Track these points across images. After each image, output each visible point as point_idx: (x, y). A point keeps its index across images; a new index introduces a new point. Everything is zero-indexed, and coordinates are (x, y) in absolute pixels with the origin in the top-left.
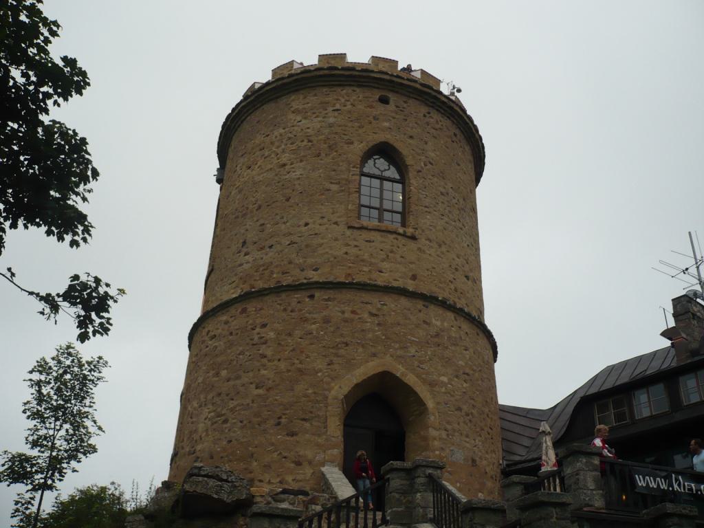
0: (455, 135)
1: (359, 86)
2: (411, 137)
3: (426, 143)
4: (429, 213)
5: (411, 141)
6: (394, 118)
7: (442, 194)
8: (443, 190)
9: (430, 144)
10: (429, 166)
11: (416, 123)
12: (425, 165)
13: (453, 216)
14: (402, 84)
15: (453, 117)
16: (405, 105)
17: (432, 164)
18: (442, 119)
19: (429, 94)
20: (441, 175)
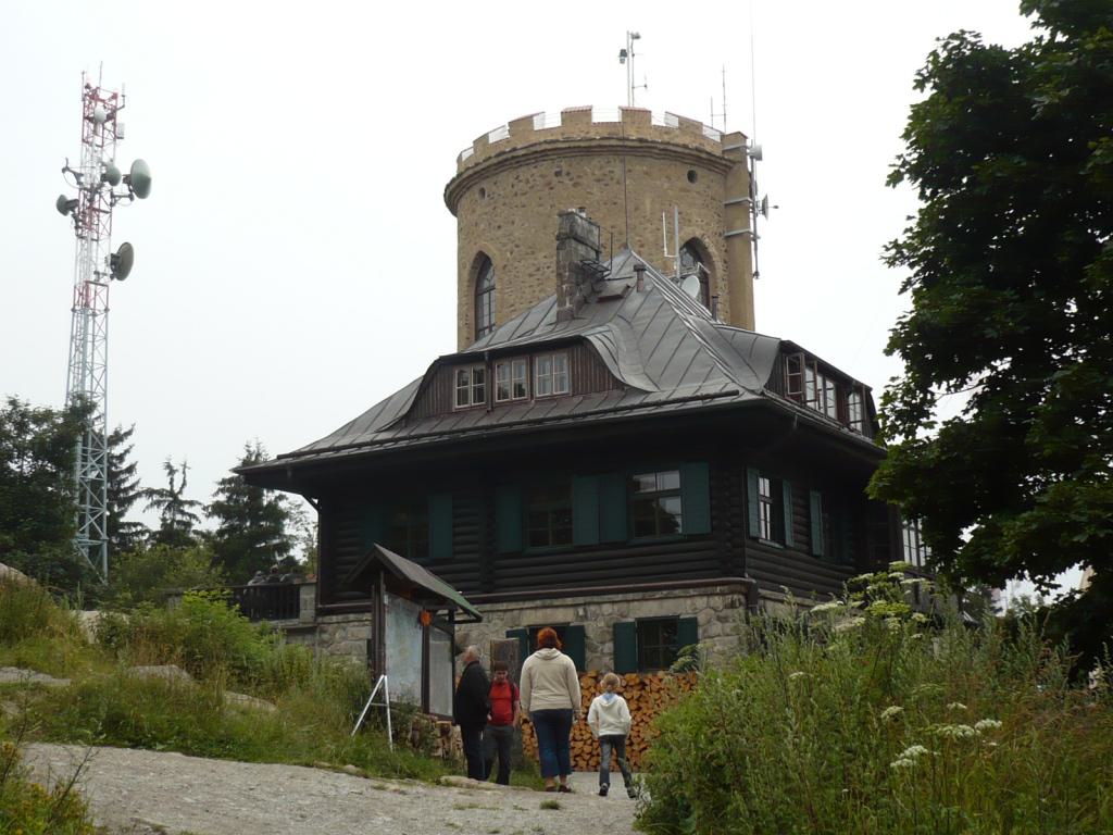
0: (558, 174)
1: (468, 189)
2: (499, 227)
3: (513, 223)
4: (515, 310)
5: (500, 233)
6: (486, 213)
7: (531, 275)
8: (532, 270)
9: (517, 219)
10: (516, 249)
11: (504, 204)
12: (511, 253)
13: (545, 292)
14: (483, 169)
15: (547, 155)
16: (494, 188)
17: (517, 246)
18: (534, 171)
19: (507, 160)
20: (529, 251)
